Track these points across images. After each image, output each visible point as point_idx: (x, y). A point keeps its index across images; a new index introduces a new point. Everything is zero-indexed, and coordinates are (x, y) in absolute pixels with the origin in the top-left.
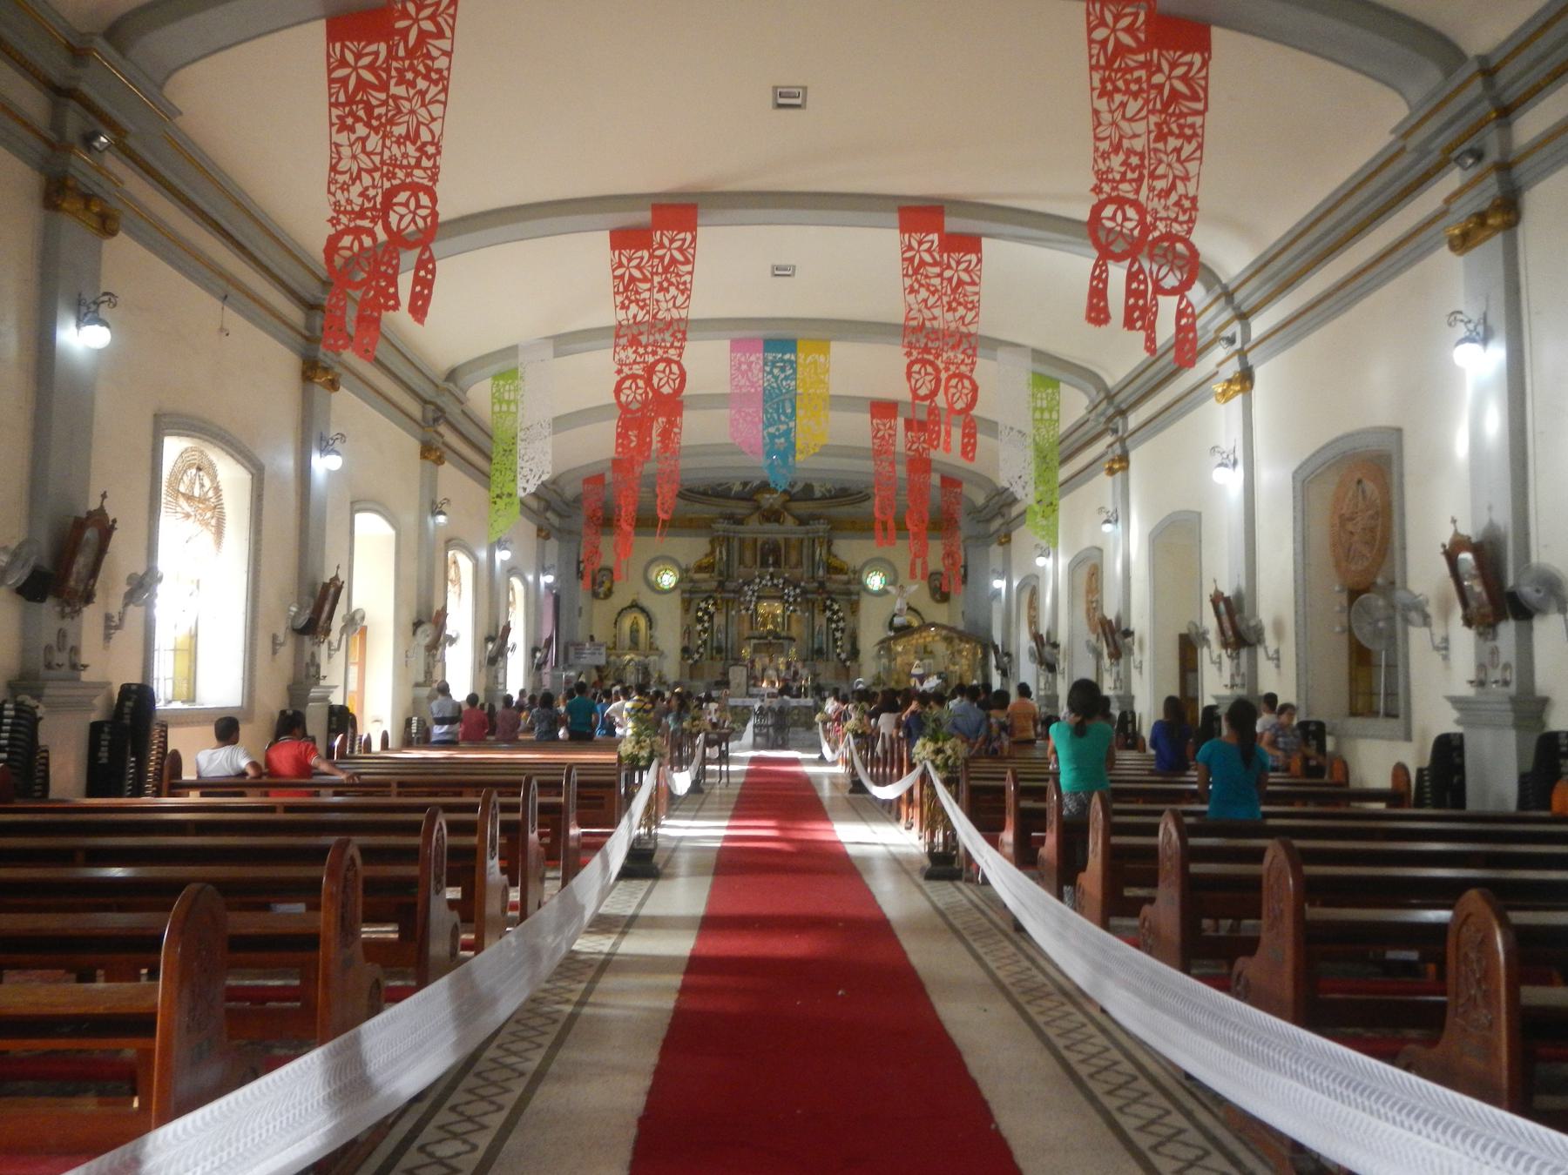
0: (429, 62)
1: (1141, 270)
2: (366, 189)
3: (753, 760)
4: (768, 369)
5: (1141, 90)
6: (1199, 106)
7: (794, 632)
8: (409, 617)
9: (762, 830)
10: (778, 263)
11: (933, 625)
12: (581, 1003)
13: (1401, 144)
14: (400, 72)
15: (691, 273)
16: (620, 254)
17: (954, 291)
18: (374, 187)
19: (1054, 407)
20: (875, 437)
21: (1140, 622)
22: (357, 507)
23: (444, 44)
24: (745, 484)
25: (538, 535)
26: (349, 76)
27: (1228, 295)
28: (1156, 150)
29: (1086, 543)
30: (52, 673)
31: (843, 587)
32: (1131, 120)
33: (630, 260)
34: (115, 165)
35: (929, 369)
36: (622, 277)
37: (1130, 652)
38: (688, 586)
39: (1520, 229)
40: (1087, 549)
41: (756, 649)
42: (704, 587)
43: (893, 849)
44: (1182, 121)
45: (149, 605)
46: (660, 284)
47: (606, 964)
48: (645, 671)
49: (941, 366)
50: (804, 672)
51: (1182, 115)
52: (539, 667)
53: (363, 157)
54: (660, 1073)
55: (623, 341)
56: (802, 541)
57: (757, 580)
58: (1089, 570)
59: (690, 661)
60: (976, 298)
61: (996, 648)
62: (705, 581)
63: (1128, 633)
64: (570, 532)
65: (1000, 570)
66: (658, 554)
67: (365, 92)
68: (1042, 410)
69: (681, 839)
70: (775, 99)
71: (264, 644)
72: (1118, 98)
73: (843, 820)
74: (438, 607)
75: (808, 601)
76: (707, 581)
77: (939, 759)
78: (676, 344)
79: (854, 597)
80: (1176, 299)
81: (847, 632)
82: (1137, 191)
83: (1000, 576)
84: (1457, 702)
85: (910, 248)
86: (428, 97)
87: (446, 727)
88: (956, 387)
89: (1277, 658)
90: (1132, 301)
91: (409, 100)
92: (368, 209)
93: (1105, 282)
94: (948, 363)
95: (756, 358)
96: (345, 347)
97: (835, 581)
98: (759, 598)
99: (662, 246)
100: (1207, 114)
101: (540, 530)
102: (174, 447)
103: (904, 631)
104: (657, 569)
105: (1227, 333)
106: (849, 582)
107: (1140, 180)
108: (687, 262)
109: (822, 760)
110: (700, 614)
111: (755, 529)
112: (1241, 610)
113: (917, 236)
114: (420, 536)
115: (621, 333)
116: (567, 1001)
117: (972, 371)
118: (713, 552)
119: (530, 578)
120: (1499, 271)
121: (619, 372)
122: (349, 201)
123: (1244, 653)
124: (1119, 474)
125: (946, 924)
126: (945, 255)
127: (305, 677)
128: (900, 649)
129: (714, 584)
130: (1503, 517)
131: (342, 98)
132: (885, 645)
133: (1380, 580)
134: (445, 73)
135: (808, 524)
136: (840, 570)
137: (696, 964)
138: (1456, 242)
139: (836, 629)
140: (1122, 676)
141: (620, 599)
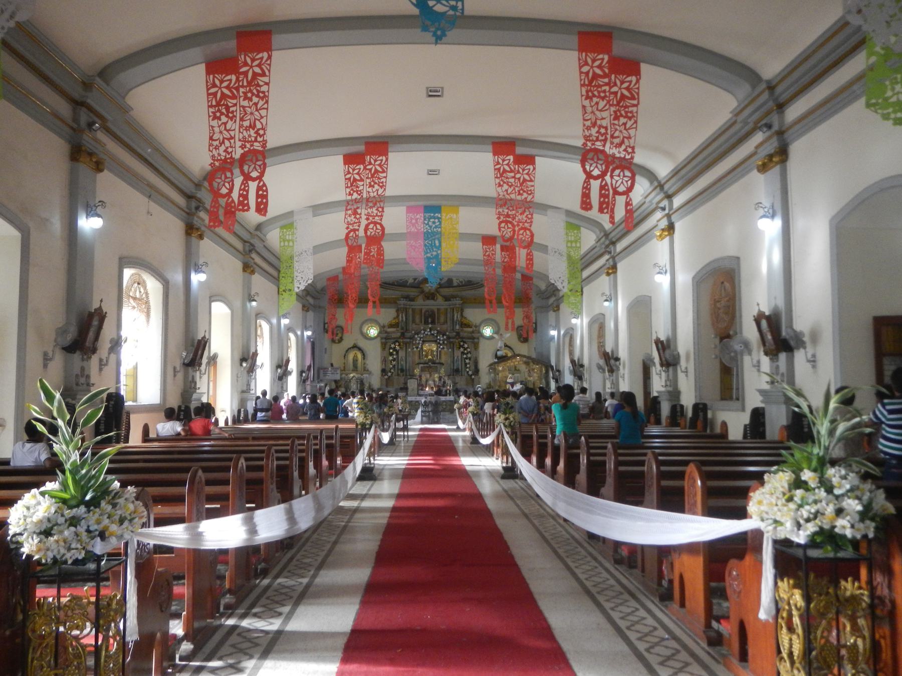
0: (258, 88)
1: (606, 184)
2: (227, 148)
3: (421, 430)
4: (426, 222)
5: (606, 96)
6: (635, 102)
7: (443, 361)
8: (238, 357)
9: (425, 461)
10: (430, 168)
11: (518, 355)
12: (348, 522)
13: (734, 119)
14: (245, 93)
15: (385, 177)
16: (349, 167)
17: (521, 185)
18: (231, 147)
19: (578, 240)
20: (484, 255)
21: (623, 353)
22: (212, 299)
23: (266, 79)
24: (415, 279)
25: (303, 310)
26: (216, 92)
27: (661, 186)
28: (614, 124)
29: (597, 312)
30: (80, 388)
31: (470, 335)
32: (601, 111)
33: (354, 170)
34: (101, 136)
35: (510, 226)
36: (349, 179)
37: (618, 369)
38: (384, 335)
40: (597, 315)
41: (422, 370)
42: (394, 336)
43: (488, 468)
44: (627, 110)
45: (118, 354)
46: (370, 183)
47: (356, 510)
48: (362, 383)
49: (516, 223)
50: (449, 382)
51: (627, 107)
52: (304, 381)
53: (225, 132)
54: (382, 541)
55: (349, 212)
56: (447, 309)
57: (423, 332)
58: (599, 326)
59: (386, 377)
60: (532, 188)
61: (552, 367)
62: (394, 332)
63: (617, 359)
64: (320, 307)
66: (366, 318)
67: (226, 100)
68: (571, 242)
69: (385, 465)
70: (427, 93)
71: (170, 372)
72: (595, 100)
73: (465, 456)
75: (451, 342)
76: (395, 333)
77: (507, 423)
78: (379, 214)
79: (476, 340)
80: (625, 196)
81: (472, 359)
82: (604, 146)
84: (762, 392)
85: (498, 163)
86: (259, 106)
87: (264, 414)
88: (523, 234)
89: (686, 372)
90: (602, 199)
91: (250, 107)
92: (228, 158)
93: (589, 190)
94: (519, 222)
95: (420, 216)
96: (218, 226)
97: (465, 332)
98: (424, 342)
99: (370, 163)
100: (639, 106)
101: (304, 306)
102: (128, 273)
103: (502, 359)
105: (662, 205)
106: (473, 332)
107: (605, 140)
108: (383, 172)
109: (458, 429)
110: (391, 351)
111: (421, 303)
112: (669, 347)
113: (502, 157)
114: (243, 314)
115: (348, 208)
116: (343, 522)
117: (530, 226)
118: (398, 316)
119: (299, 333)
120: (778, 185)
121: (347, 228)
122: (219, 155)
123: (671, 369)
124: (612, 276)
125: (508, 495)
126: (517, 166)
127: (189, 388)
128: (500, 369)
129: (399, 334)
130: (781, 303)
131: (214, 103)
132: (492, 366)
133: (731, 333)
134: (267, 94)
136: (469, 326)
137: (394, 509)
138: (761, 168)
139: (466, 358)
140: (614, 382)
141: (348, 342)
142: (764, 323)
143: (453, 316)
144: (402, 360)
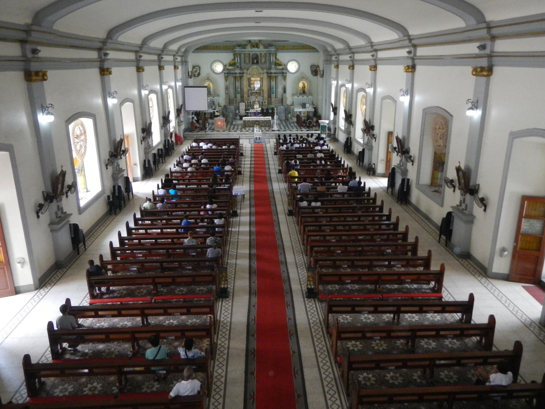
38: (226, 71)
39: (492, 77)
65: (335, 78)
74: (148, 122)
79: (285, 75)
83: (335, 80)
104: (215, 65)
106: (283, 69)
118: (234, 59)
135: (268, 48)
136: (280, 65)
142: (461, 174)
143: (270, 58)
144: (238, 87)
